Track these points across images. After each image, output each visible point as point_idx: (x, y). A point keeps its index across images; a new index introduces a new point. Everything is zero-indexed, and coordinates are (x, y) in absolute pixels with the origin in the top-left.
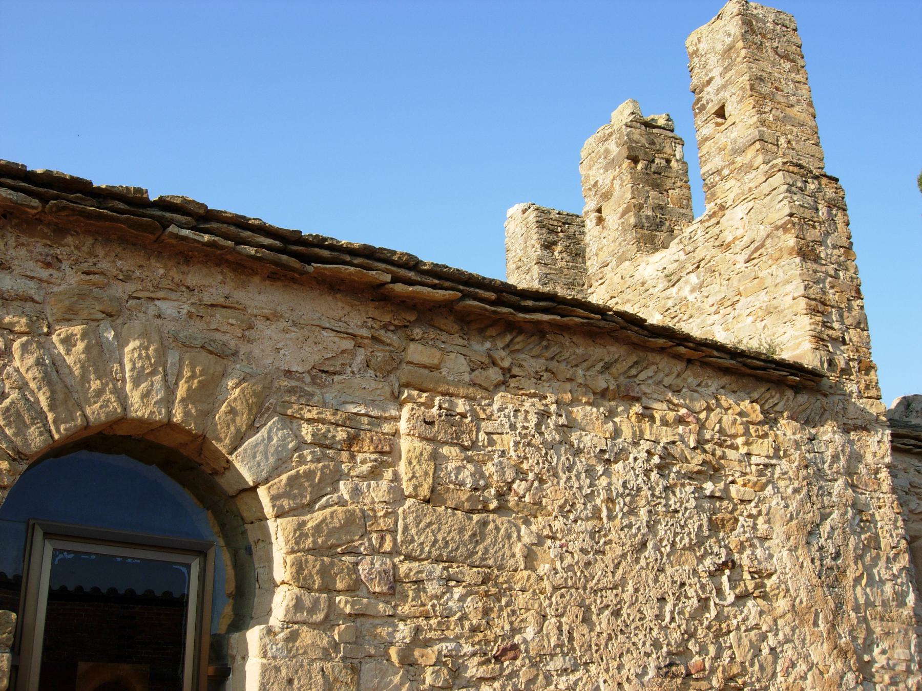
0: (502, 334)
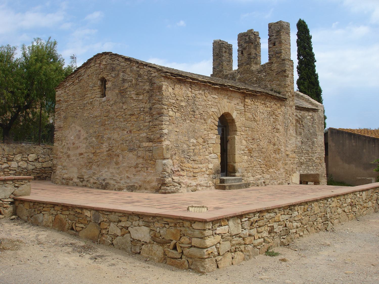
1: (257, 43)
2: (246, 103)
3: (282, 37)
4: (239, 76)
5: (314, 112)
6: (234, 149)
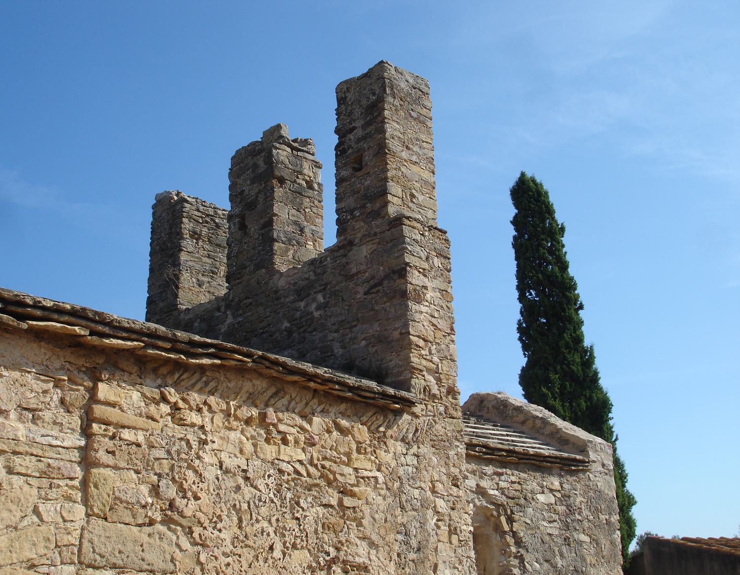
0: (171, 373)
1: (307, 182)
4: (230, 320)
5: (572, 473)
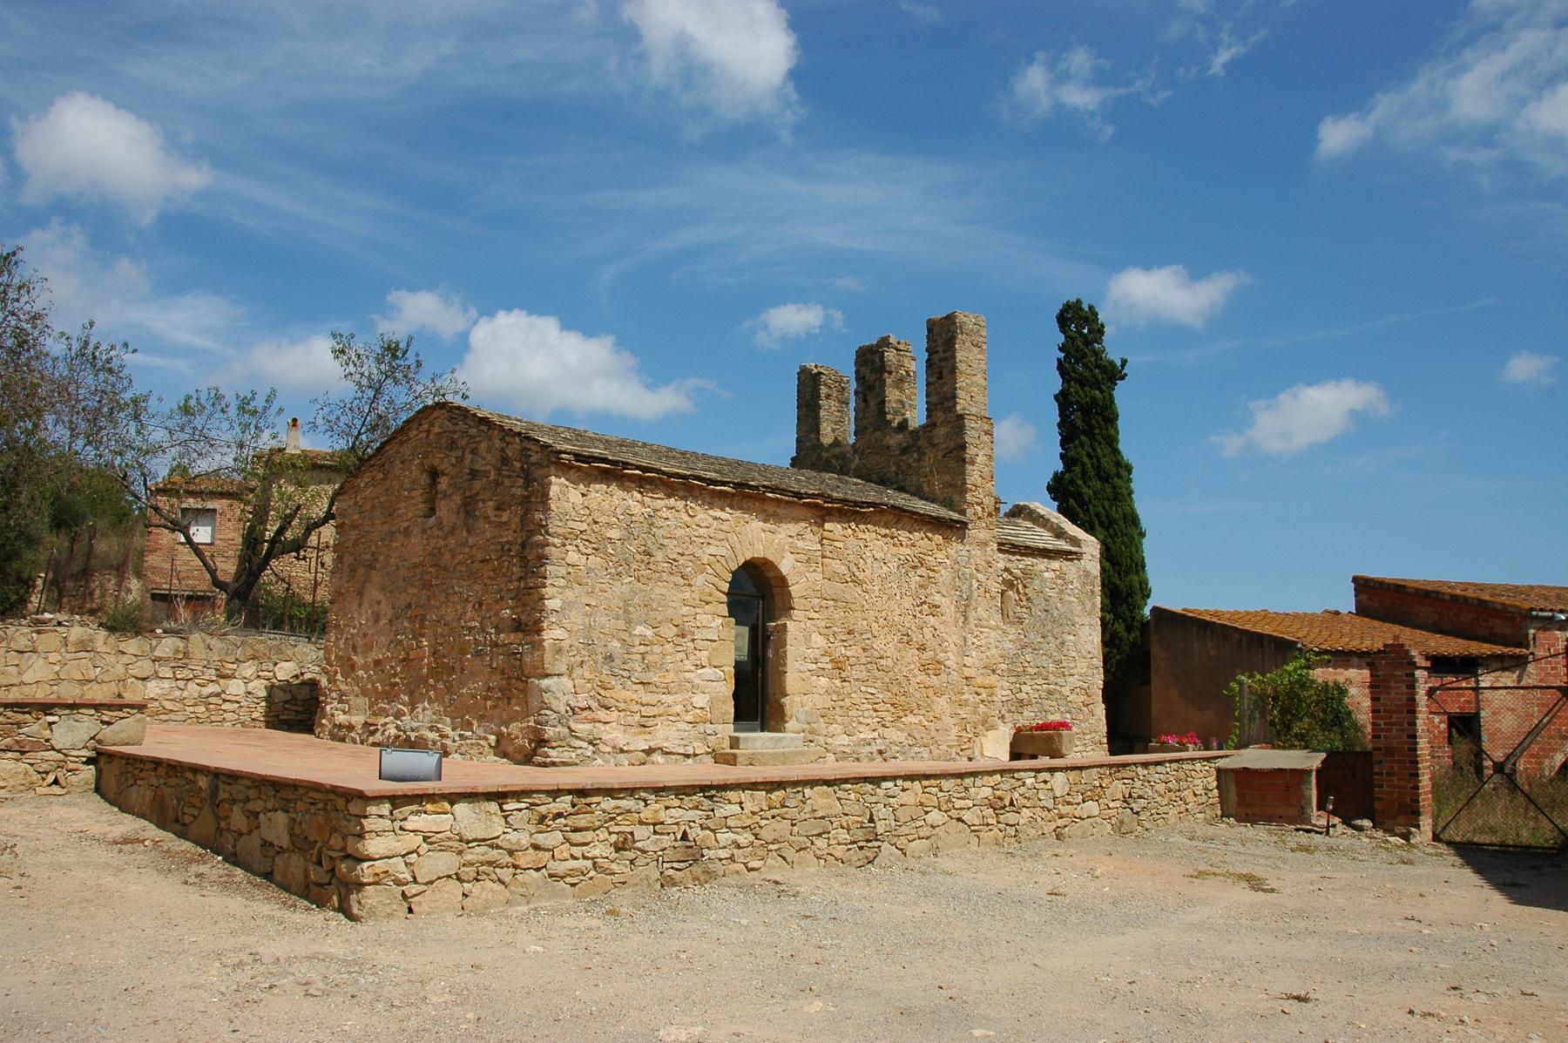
2: (826, 534)
3: (959, 356)
6: (784, 657)
